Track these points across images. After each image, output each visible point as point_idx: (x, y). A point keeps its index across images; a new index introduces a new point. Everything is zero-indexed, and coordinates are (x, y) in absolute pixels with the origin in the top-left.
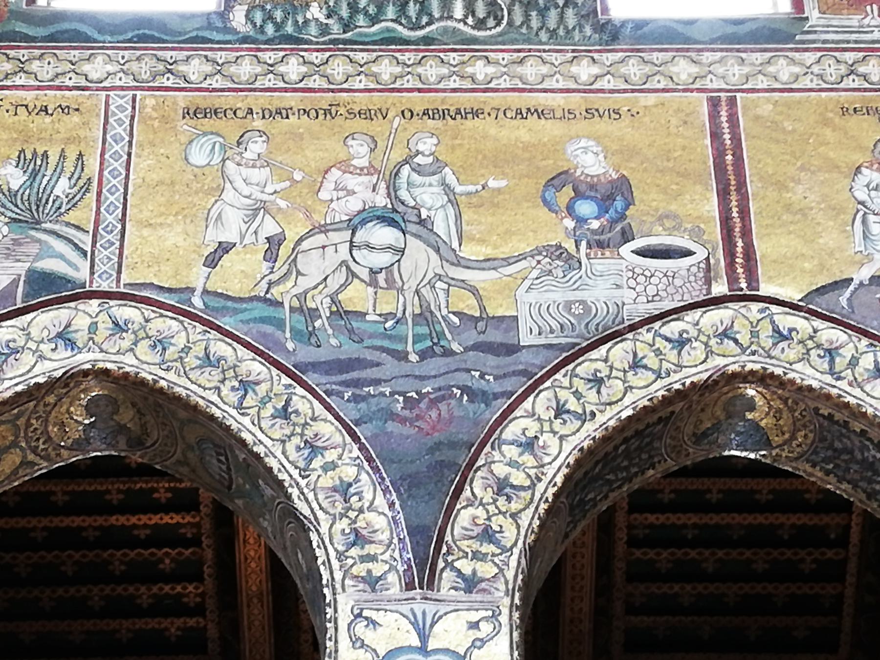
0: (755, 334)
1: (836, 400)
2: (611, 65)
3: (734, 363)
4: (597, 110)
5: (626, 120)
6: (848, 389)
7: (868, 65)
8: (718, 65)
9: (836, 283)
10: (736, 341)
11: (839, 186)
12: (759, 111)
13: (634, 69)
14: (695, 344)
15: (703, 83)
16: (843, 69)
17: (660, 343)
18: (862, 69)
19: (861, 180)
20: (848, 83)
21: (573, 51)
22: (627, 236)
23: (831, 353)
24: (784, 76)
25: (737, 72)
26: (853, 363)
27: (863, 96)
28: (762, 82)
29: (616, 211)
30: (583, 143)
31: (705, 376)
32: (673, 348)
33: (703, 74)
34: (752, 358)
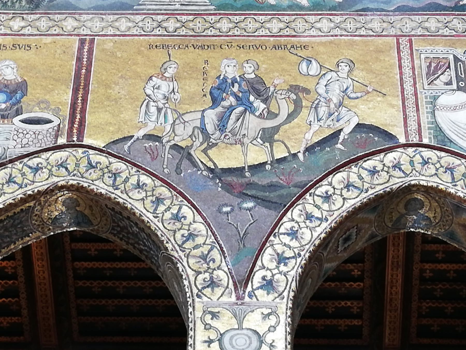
0: (77, 165)
1: (113, 201)
2: (32, 21)
3: (63, 180)
4: (19, 45)
5: (33, 50)
6: (120, 194)
7: (169, 22)
8: (89, 22)
9: (125, 138)
10: (66, 169)
11: (138, 87)
12: (105, 47)
13: (43, 23)
14: (44, 170)
15: (79, 31)
16: (155, 24)
17: (26, 169)
18: (165, 25)
19: (152, 83)
20: (157, 32)
21: (13, 14)
22: (18, 112)
23: (115, 175)
24: (123, 28)
25: (98, 25)
26: (126, 180)
27: (162, 39)
28: (110, 31)
29: (16, 99)
30: (7, 63)
31: (46, 187)
32: (31, 172)
33: (80, 26)
34: (73, 178)
